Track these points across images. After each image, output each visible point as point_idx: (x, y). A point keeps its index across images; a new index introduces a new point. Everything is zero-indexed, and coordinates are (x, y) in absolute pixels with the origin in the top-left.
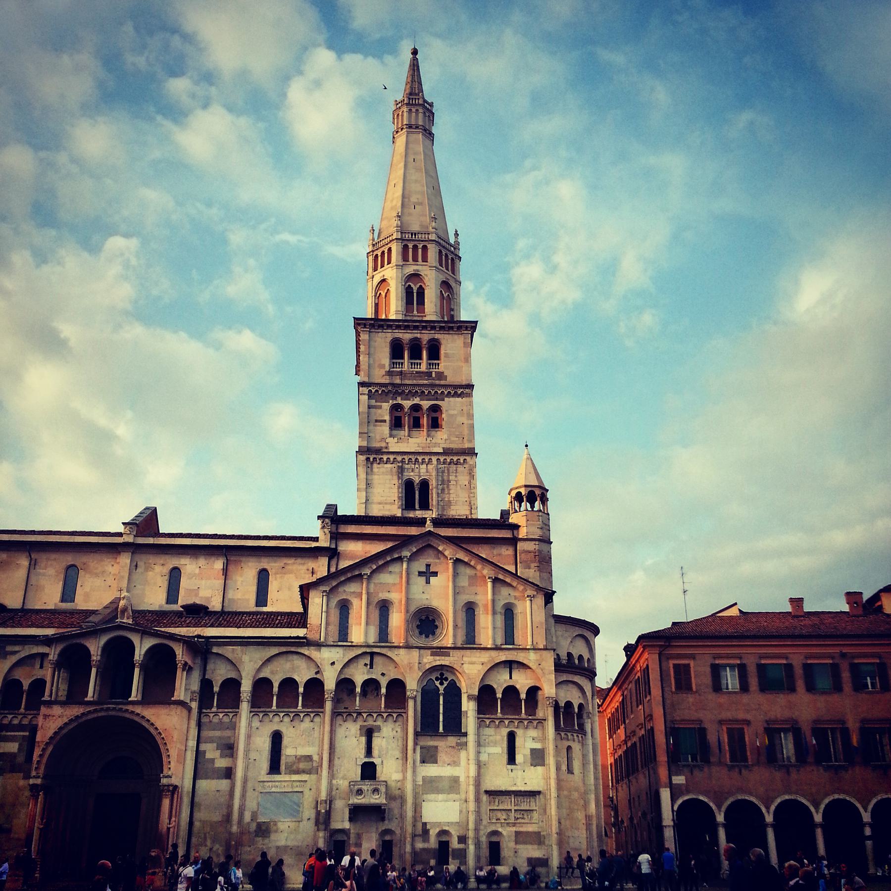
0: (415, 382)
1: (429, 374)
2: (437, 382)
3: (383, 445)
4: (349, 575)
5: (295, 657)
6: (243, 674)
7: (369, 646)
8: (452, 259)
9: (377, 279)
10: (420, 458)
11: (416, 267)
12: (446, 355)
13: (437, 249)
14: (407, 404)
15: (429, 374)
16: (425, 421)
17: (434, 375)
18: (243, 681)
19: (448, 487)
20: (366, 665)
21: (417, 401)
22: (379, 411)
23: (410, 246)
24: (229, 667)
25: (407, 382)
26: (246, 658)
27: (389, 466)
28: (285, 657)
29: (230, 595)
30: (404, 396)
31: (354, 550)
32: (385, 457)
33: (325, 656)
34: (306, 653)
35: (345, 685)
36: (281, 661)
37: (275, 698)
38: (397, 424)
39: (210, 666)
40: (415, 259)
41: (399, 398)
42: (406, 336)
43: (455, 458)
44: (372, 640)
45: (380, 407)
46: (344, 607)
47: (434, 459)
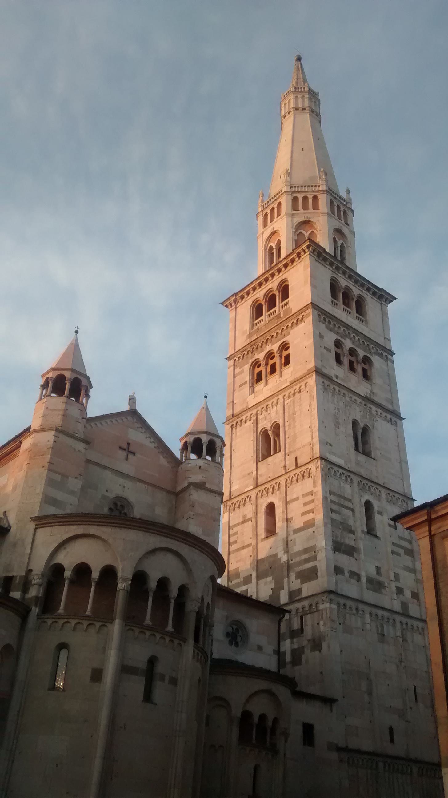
10: (270, 403)
11: (272, 227)
13: (290, 198)
14: (261, 356)
15: (278, 317)
17: (282, 315)
19: (294, 420)
22: (243, 375)
23: (268, 211)
27: (249, 423)
32: (244, 417)
40: (272, 220)
41: (256, 354)
42: (260, 294)
45: (242, 372)
47: (281, 397)
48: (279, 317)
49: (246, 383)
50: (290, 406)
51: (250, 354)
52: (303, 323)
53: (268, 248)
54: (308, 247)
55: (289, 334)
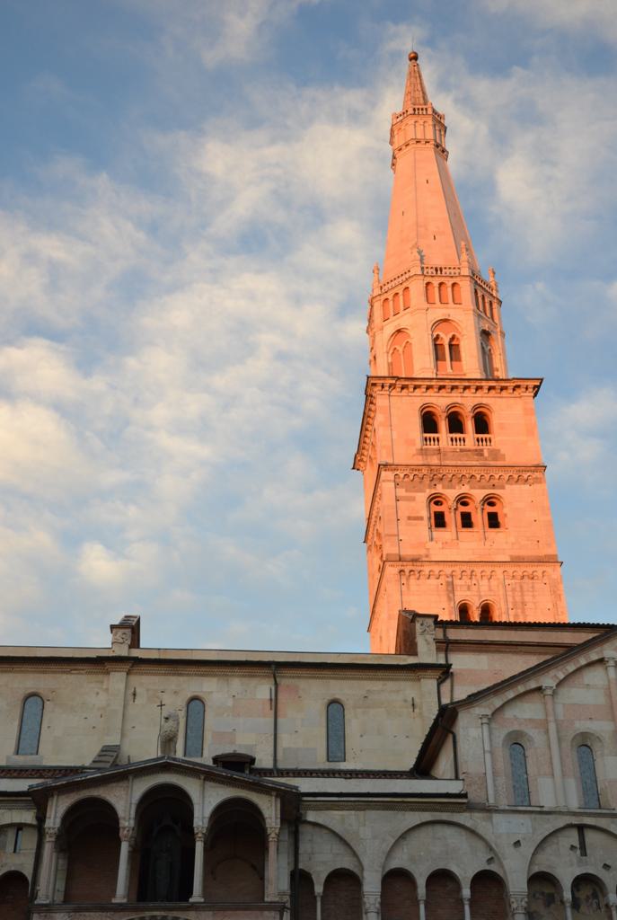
0: (459, 463)
1: (480, 453)
2: (492, 463)
3: (422, 552)
4: (521, 689)
5: (448, 832)
6: (365, 862)
7: (574, 814)
8: (491, 304)
9: (390, 329)
10: (478, 570)
12: (502, 426)
14: (451, 494)
16: (479, 518)
17: (486, 454)
18: (366, 874)
20: (573, 847)
21: (465, 489)
22: (413, 504)
23: (435, 282)
24: (338, 848)
25: (448, 463)
26: (365, 832)
27: (433, 581)
28: (430, 829)
29: (285, 741)
30: (446, 482)
31: (474, 670)
32: (426, 569)
33: (502, 829)
34: (468, 824)
35: (542, 881)
36: (424, 836)
37: (422, 907)
38: (440, 521)
39: (304, 847)
42: (441, 402)
43: (530, 569)
44: (574, 803)
45: (413, 499)
46: (516, 742)
47: (499, 570)
48: (482, 455)
49: (421, 518)
50: (514, 590)
51: (426, 480)
52: (527, 486)
53: (435, 336)
54: (535, 387)
55: (503, 488)
